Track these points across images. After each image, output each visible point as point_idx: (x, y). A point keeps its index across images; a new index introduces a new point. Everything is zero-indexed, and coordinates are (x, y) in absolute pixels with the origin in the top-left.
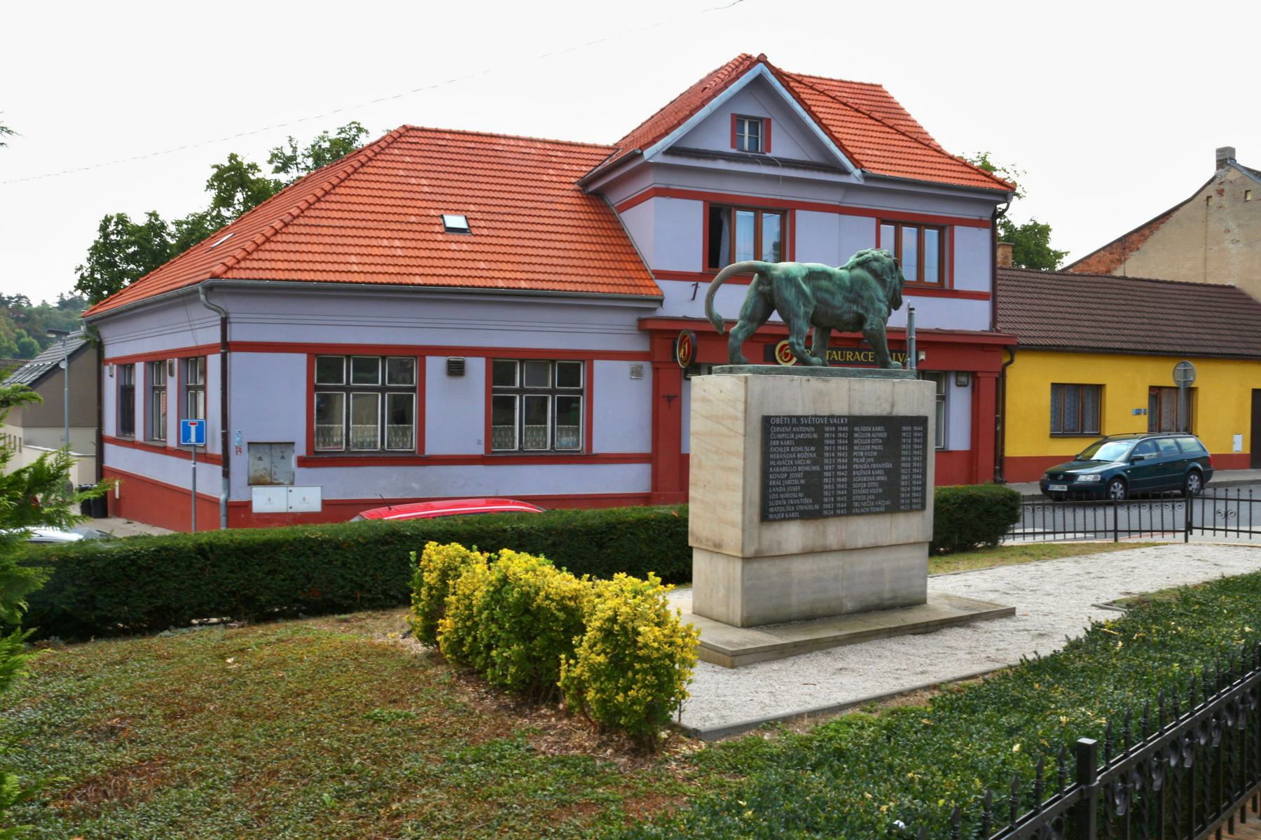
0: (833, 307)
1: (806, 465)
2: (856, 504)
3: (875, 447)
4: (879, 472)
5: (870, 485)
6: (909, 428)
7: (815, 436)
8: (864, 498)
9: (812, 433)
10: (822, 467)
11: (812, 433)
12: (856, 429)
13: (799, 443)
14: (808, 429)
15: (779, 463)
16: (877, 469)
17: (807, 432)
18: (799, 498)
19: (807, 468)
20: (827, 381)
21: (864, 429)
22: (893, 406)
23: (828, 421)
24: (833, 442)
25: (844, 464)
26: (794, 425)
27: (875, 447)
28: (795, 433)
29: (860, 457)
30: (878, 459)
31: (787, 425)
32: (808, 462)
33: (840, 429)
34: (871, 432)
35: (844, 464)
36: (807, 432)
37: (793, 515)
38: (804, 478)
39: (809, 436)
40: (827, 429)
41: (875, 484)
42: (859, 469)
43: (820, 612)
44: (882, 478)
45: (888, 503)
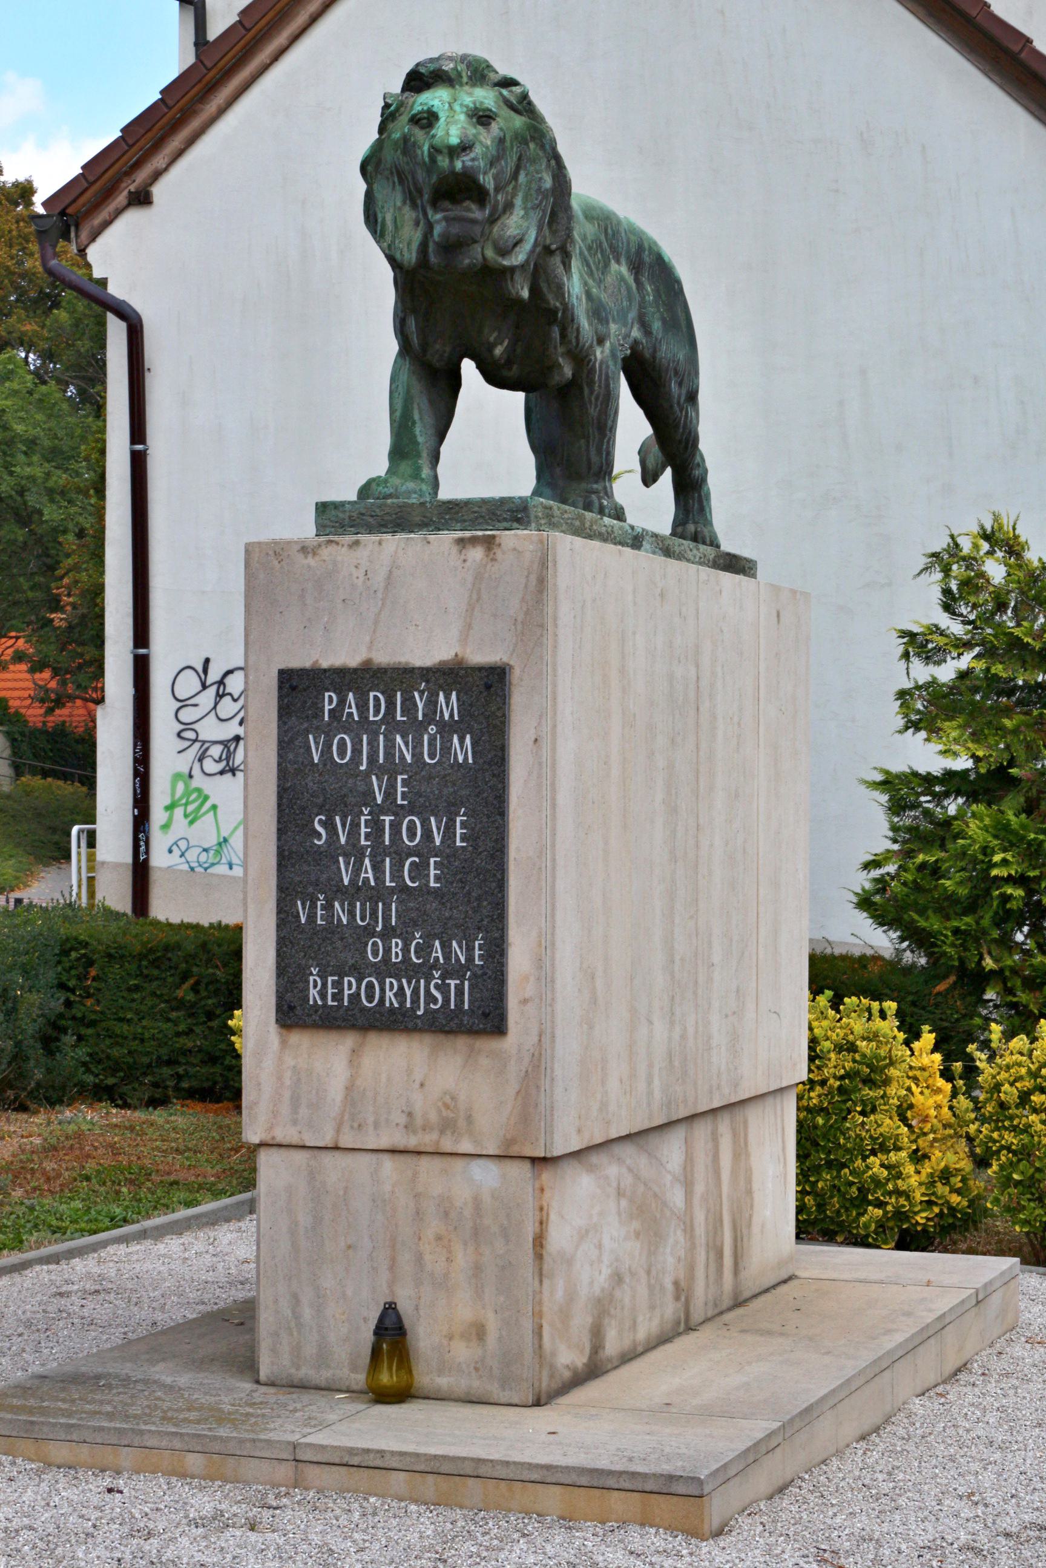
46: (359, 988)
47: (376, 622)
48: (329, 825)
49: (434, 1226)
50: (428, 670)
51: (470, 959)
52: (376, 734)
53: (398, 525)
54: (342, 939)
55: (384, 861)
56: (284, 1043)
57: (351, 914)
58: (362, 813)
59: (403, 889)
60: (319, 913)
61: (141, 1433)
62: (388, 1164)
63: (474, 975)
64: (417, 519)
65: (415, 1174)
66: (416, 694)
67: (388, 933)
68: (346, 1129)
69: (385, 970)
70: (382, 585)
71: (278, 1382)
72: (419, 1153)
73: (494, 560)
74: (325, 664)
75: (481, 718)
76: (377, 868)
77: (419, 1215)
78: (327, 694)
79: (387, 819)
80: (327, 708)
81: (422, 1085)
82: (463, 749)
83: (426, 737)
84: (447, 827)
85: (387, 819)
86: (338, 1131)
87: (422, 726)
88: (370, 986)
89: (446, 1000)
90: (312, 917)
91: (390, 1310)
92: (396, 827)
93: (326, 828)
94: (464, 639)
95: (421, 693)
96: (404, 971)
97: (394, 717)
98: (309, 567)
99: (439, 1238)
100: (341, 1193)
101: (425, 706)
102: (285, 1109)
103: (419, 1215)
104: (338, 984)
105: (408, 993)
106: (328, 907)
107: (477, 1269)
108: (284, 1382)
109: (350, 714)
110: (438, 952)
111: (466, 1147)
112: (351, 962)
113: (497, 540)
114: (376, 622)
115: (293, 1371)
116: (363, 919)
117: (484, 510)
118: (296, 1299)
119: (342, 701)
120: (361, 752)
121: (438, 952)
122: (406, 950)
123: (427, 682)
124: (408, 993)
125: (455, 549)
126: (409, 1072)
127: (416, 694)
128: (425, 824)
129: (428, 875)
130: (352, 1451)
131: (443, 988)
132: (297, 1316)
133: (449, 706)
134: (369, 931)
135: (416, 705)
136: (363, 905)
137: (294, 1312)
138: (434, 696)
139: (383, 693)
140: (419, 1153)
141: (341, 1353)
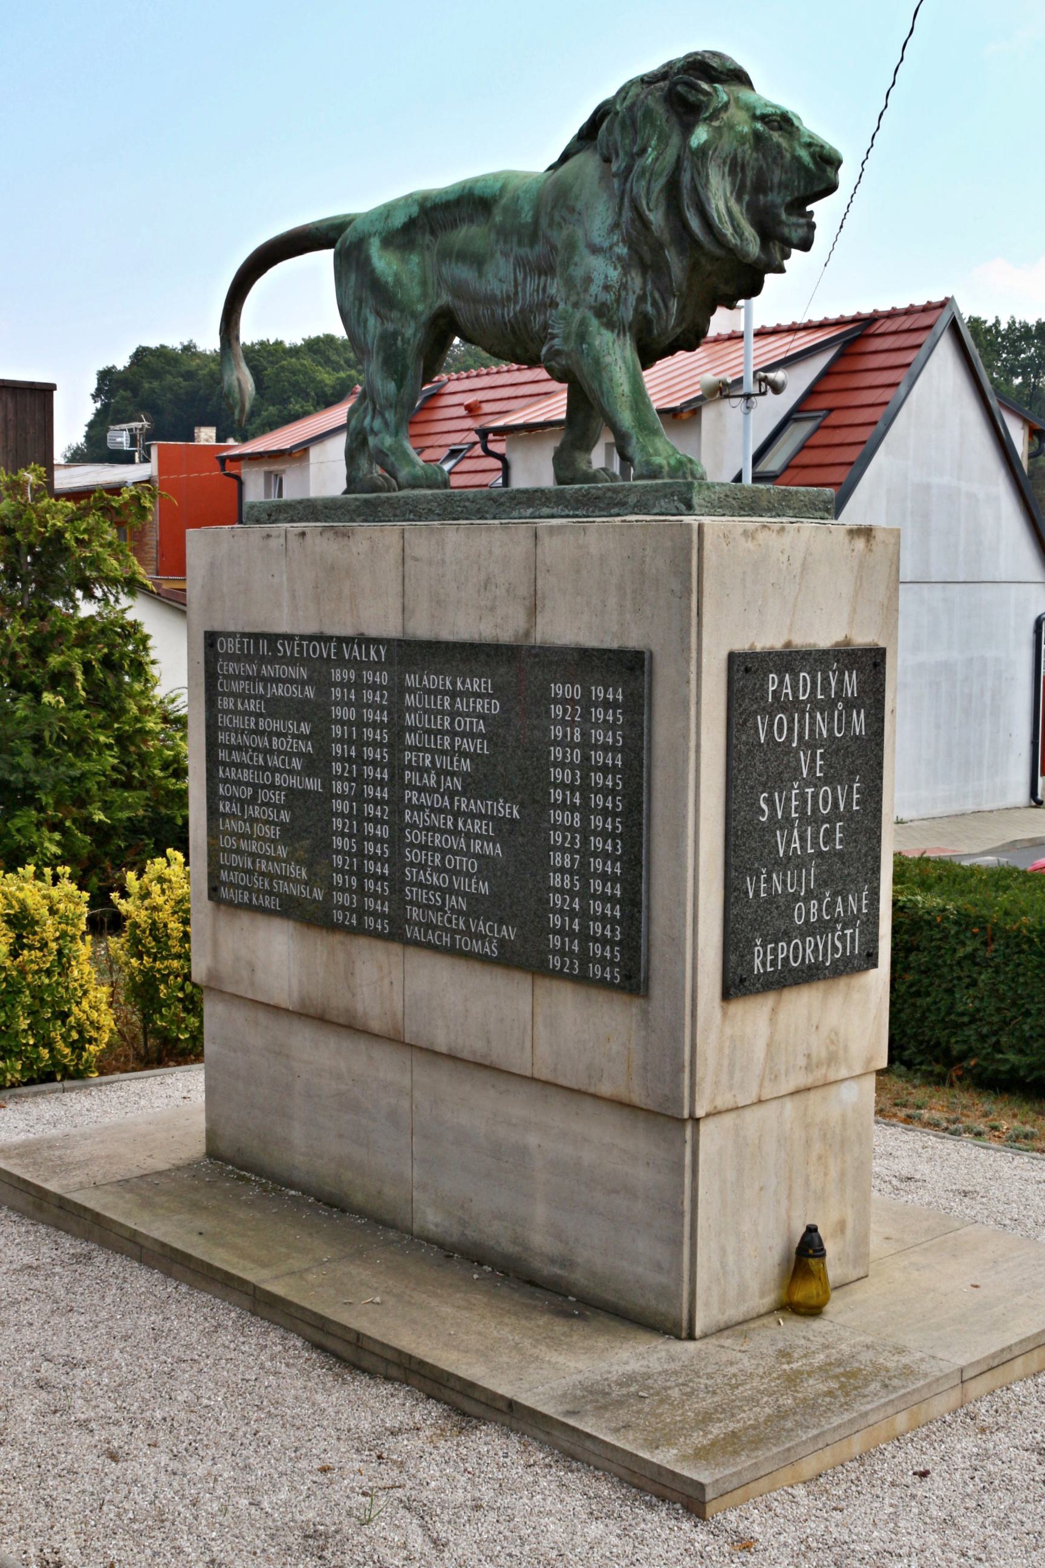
0: (490, 300)
1: (291, 772)
2: (415, 913)
3: (467, 745)
4: (477, 826)
5: (454, 862)
6: (575, 691)
7: (310, 693)
8: (436, 899)
9: (303, 683)
10: (327, 786)
11: (303, 683)
12: (411, 680)
13: (275, 708)
14: (292, 672)
15: (236, 757)
16: (473, 816)
17: (292, 681)
18: (277, 859)
19: (294, 782)
20: (346, 535)
21: (432, 681)
22: (533, 611)
23: (339, 652)
24: (351, 714)
25: (381, 783)
26: (263, 660)
27: (467, 745)
28: (267, 680)
29: (422, 770)
30: (473, 787)
31: (248, 659)
32: (297, 764)
33: (368, 676)
34: (454, 694)
35: (381, 783)
36: (292, 681)
37: (268, 902)
38: (288, 806)
39: (295, 692)
40: (337, 675)
41: (470, 865)
42: (421, 808)
43: (358, 1198)
44: (489, 849)
45: (509, 933)
46: (788, 951)
47: (795, 605)
48: (770, 801)
49: (817, 1147)
50: (825, 652)
51: (859, 909)
52: (803, 712)
53: (752, 509)
54: (777, 908)
55: (806, 830)
56: (725, 1014)
57: (784, 883)
58: (792, 786)
59: (820, 854)
60: (763, 886)
61: (866, 1414)
62: (789, 1105)
63: (862, 923)
64: (765, 504)
65: (807, 1107)
66: (831, 674)
67: (810, 895)
68: (766, 1083)
69: (809, 929)
70: (799, 570)
71: (709, 1332)
72: (809, 1089)
73: (871, 550)
74: (759, 647)
75: (871, 695)
76: (803, 839)
77: (808, 1143)
78: (771, 676)
79: (810, 791)
80: (771, 689)
81: (817, 1028)
82: (859, 723)
83: (836, 713)
84: (848, 795)
85: (810, 791)
86: (761, 1086)
87: (831, 704)
88: (796, 947)
89: (845, 948)
90: (757, 892)
91: (811, 1230)
92: (815, 796)
93: (768, 805)
94: (851, 622)
95: (834, 672)
96: (823, 927)
97: (816, 696)
98: (749, 551)
99: (820, 1158)
100: (757, 1142)
101: (837, 683)
102: (724, 1079)
103: (808, 1143)
104: (774, 951)
105: (821, 947)
106: (769, 880)
107: (842, 1174)
108: (713, 1330)
109: (787, 694)
110: (840, 909)
111: (843, 1073)
112: (783, 928)
113: (874, 533)
114: (795, 605)
115: (720, 1317)
116: (792, 887)
117: (807, 499)
118: (723, 1250)
119: (781, 682)
120: (793, 730)
121: (840, 909)
122: (820, 910)
123: (838, 662)
124: (821, 947)
125: (847, 539)
126: (809, 1018)
127: (831, 674)
128: (834, 791)
129: (835, 839)
130: (994, 1356)
131: (842, 938)
132: (723, 1265)
133: (851, 684)
134: (796, 897)
135: (830, 684)
136: (792, 873)
137: (721, 1263)
138: (842, 674)
139: (809, 674)
140: (809, 1089)
141: (754, 1286)
